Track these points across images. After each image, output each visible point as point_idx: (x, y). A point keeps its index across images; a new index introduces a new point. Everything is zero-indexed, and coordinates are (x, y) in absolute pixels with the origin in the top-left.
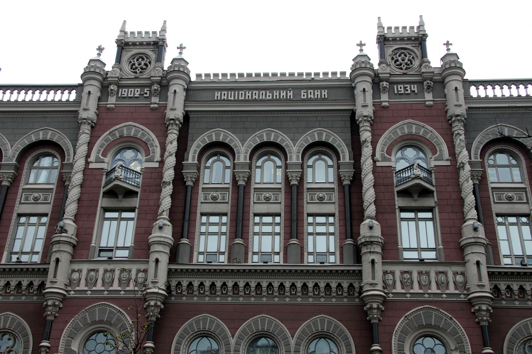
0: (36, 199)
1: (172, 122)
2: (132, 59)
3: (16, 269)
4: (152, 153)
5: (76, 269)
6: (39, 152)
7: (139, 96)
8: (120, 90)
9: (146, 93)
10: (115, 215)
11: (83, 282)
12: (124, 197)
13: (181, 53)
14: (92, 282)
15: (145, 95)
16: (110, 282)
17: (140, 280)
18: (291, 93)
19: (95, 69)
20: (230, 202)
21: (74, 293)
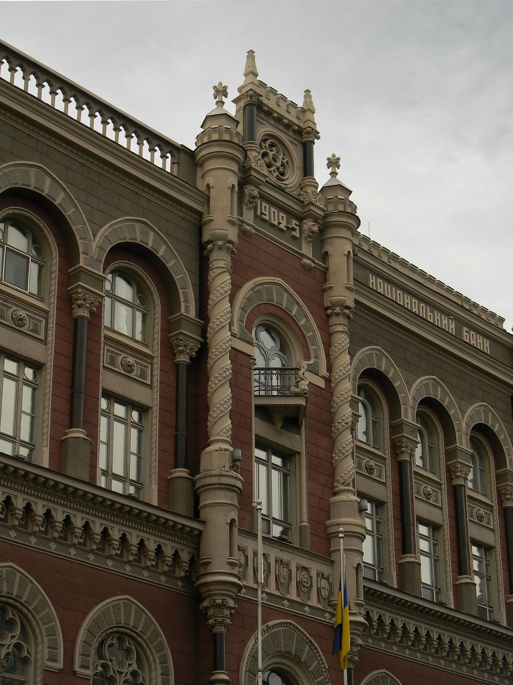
7: (285, 229)
12: (282, 427)
13: (334, 174)
20: (389, 484)
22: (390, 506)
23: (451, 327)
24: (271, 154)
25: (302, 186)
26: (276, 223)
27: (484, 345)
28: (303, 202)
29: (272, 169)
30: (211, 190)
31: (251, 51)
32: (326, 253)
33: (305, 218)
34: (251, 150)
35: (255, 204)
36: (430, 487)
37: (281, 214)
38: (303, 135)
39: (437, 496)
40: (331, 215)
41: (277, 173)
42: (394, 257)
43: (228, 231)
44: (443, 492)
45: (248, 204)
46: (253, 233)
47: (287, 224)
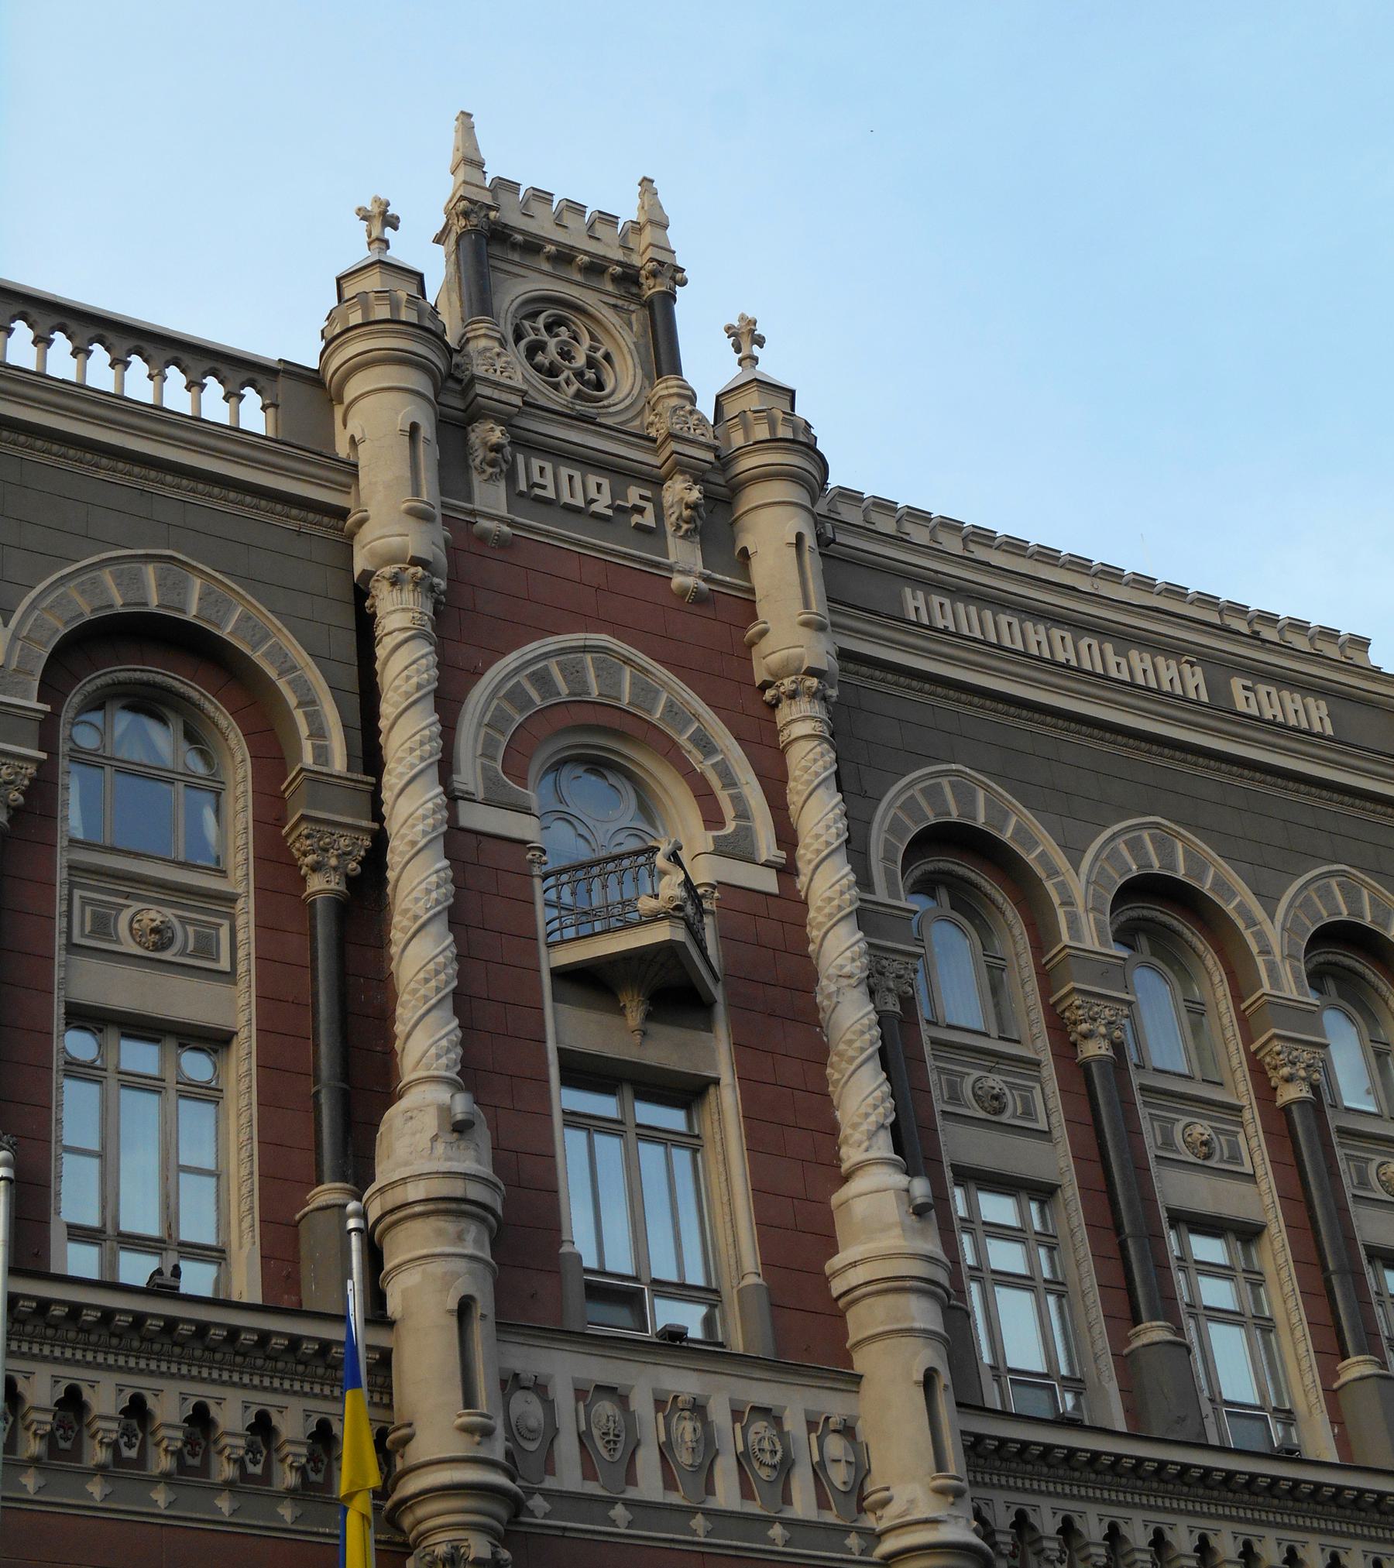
0: (162, 937)
1: (813, 682)
2: (526, 317)
3: (265, 1336)
4: (737, 817)
5: (527, 1376)
6: (122, 676)
7: (610, 512)
8: (520, 459)
9: (640, 510)
10: (603, 1105)
11: (567, 1448)
14: (618, 1455)
15: (636, 519)
16: (701, 1464)
17: (839, 1475)
18: (1199, 678)
19: (366, 310)
21: (547, 1506)
22: (1071, 1192)
23: (1195, 682)
24: (552, 344)
25: (652, 403)
26: (579, 502)
27: (1317, 715)
28: (654, 440)
29: (561, 378)
30: (360, 448)
31: (645, 179)
32: (744, 552)
33: (669, 476)
34: (476, 337)
35: (504, 467)
36: (1206, 1123)
37: (593, 480)
38: (642, 284)
39: (1234, 1147)
40: (737, 457)
41: (576, 385)
42: (983, 536)
43: (407, 535)
44: (1250, 1129)
45: (486, 467)
46: (507, 535)
47: (613, 499)
